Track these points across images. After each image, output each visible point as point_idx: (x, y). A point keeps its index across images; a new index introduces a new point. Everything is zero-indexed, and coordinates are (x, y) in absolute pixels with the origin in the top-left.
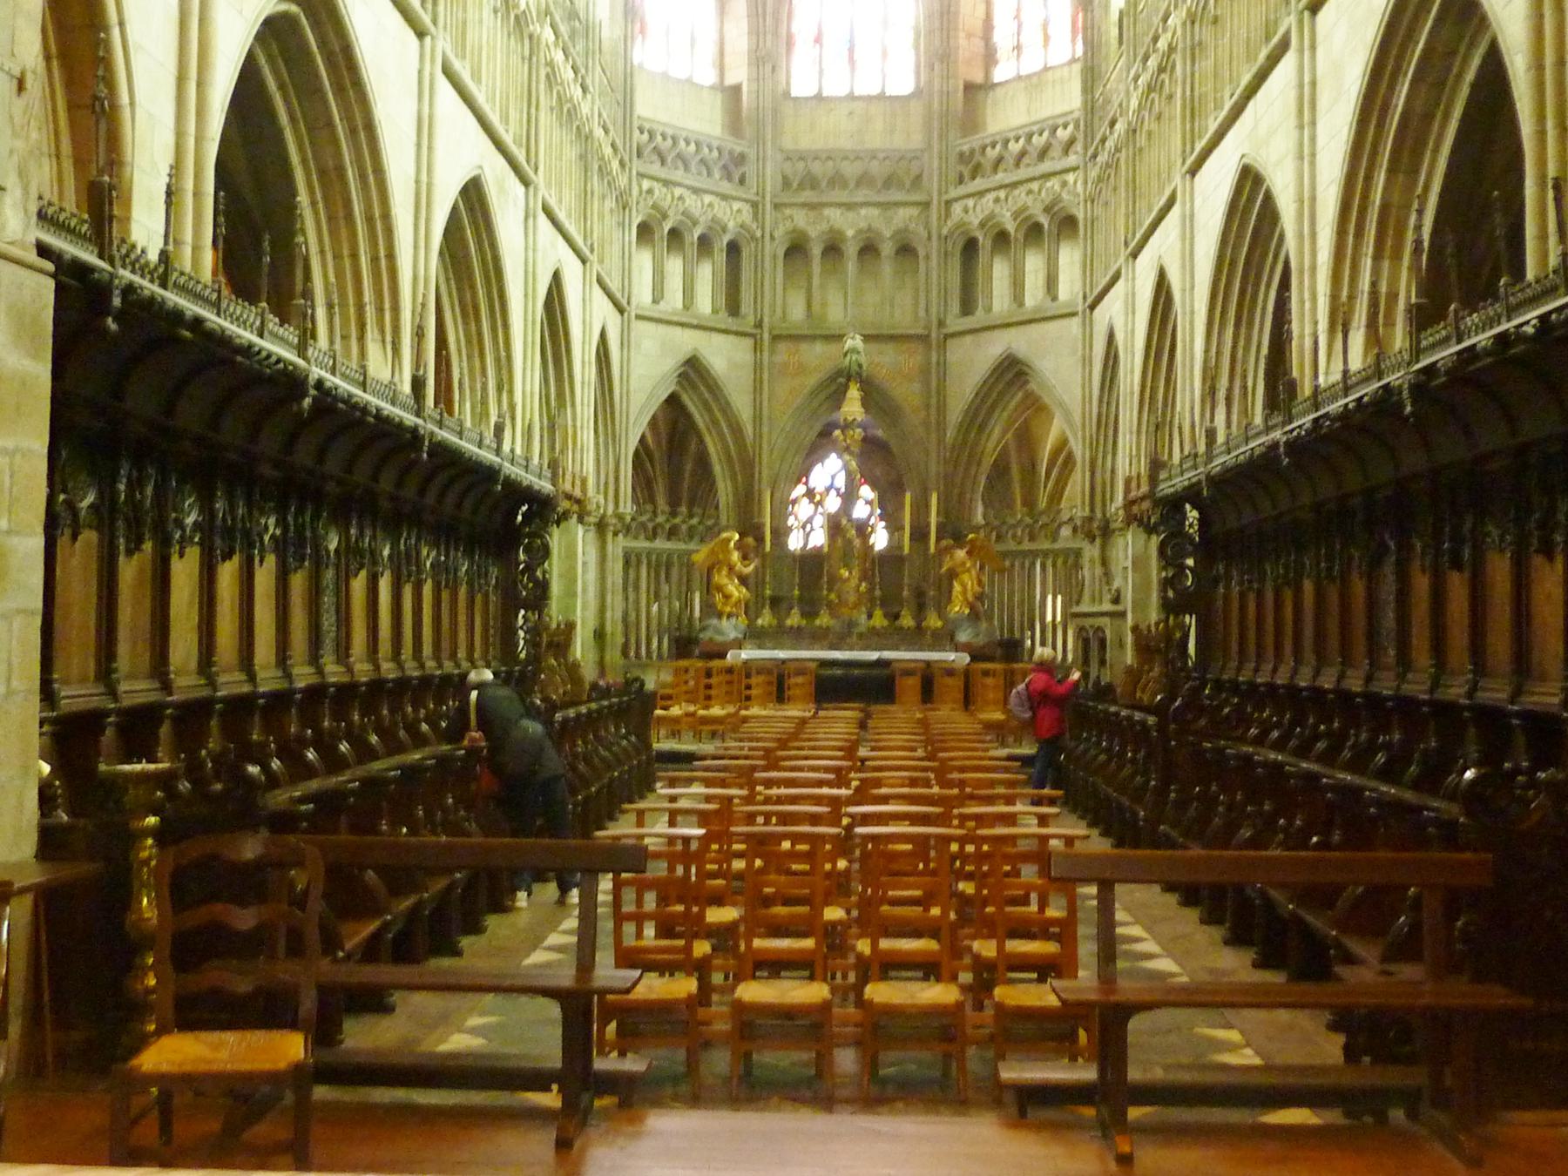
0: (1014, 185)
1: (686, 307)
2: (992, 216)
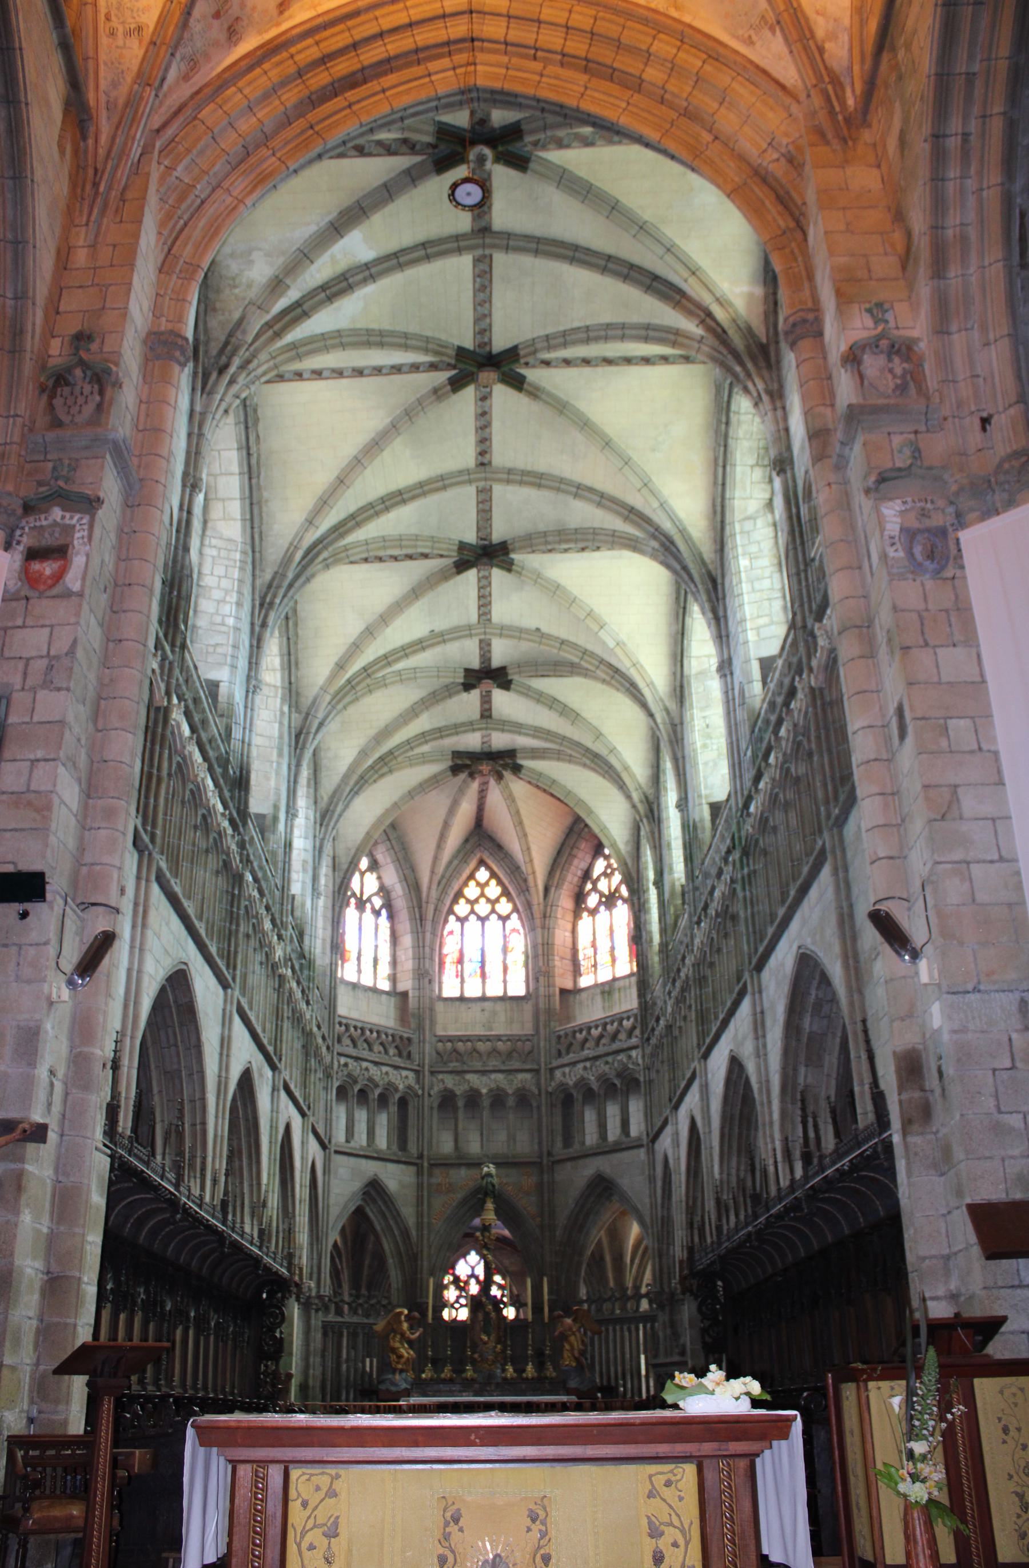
0: (596, 1058)
1: (369, 1145)
2: (583, 1079)
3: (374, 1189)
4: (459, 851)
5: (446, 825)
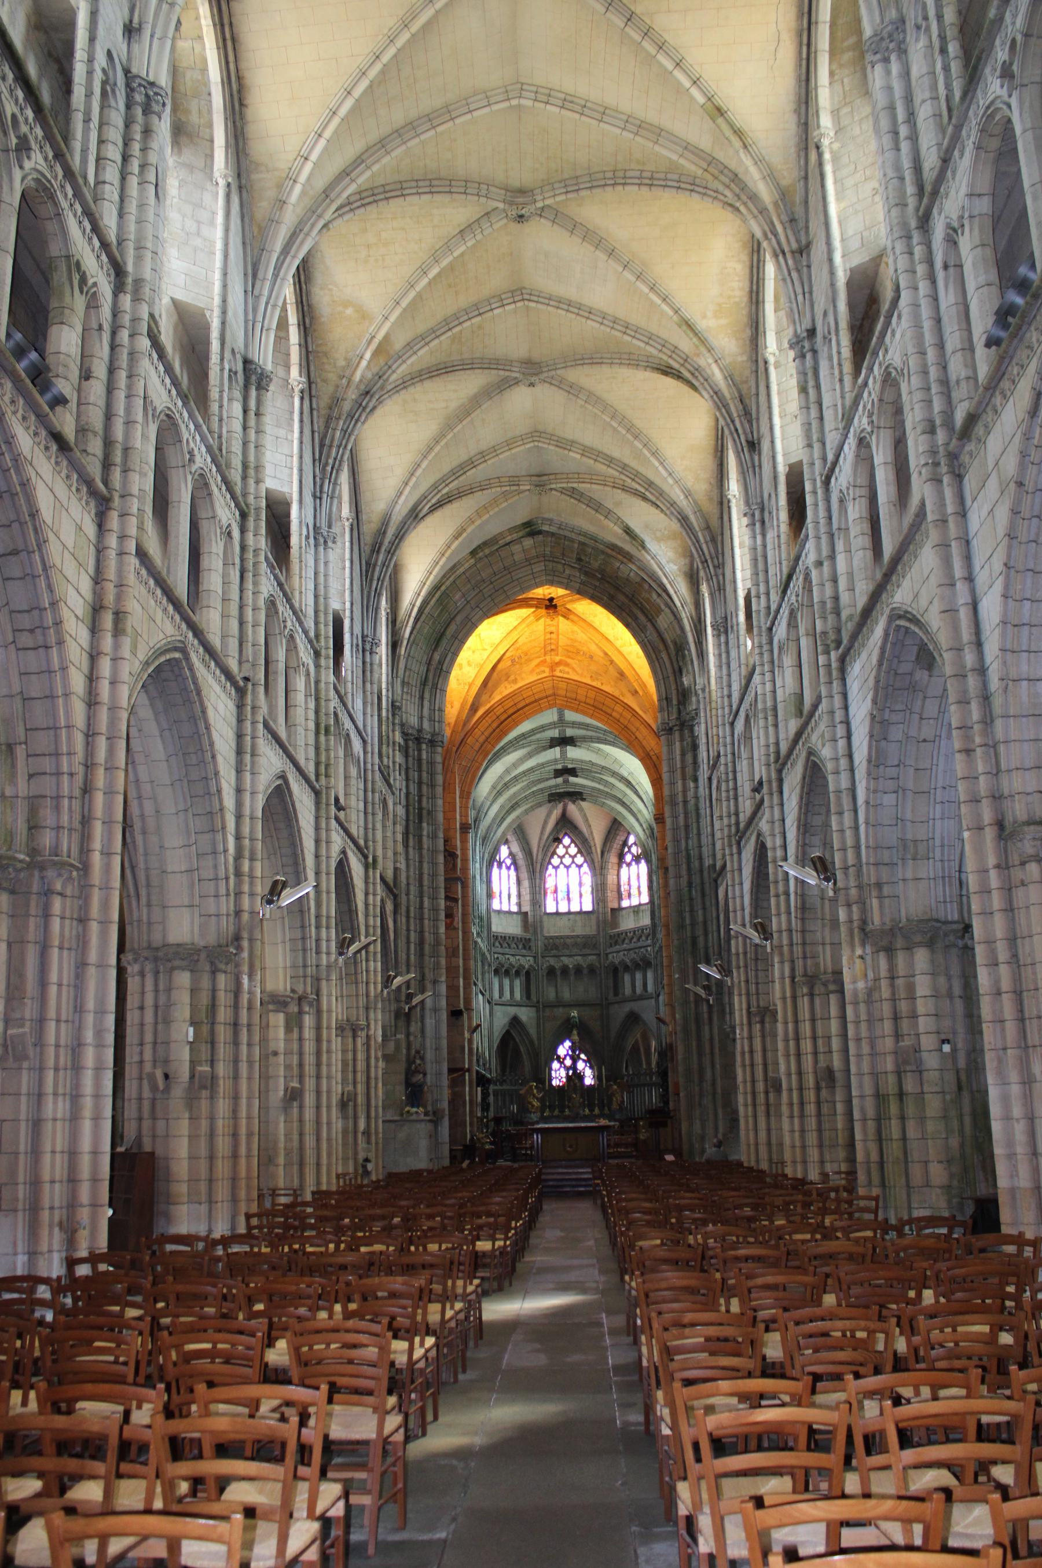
3: (515, 1021)
5: (545, 823)
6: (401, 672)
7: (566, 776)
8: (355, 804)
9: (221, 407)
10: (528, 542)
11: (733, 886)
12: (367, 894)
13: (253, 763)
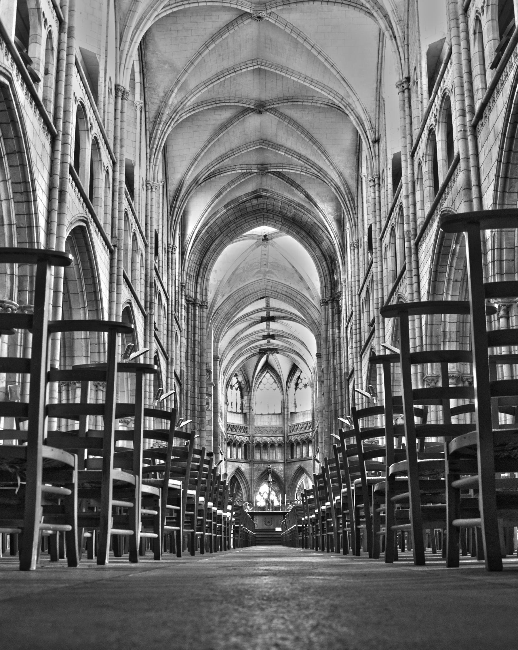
0: (300, 434)
4: (261, 370)
6: (186, 268)
7: (269, 339)
8: (163, 329)
9: (104, 105)
10: (255, 202)
11: (357, 378)
12: (167, 378)
13: (118, 288)
